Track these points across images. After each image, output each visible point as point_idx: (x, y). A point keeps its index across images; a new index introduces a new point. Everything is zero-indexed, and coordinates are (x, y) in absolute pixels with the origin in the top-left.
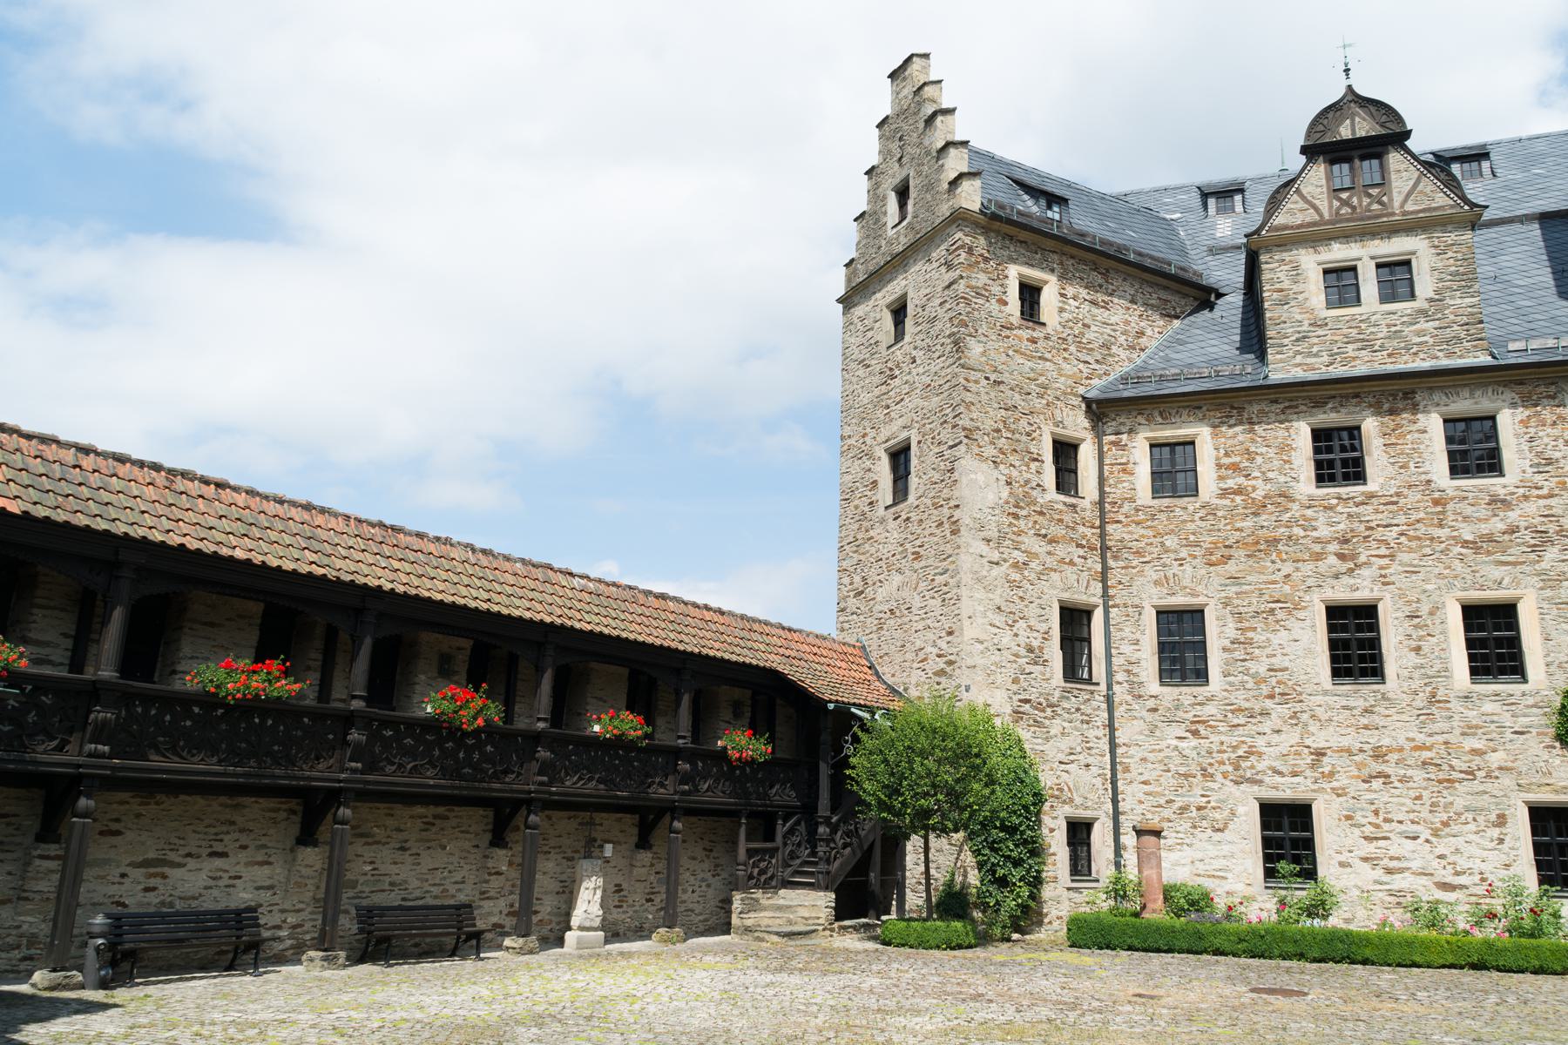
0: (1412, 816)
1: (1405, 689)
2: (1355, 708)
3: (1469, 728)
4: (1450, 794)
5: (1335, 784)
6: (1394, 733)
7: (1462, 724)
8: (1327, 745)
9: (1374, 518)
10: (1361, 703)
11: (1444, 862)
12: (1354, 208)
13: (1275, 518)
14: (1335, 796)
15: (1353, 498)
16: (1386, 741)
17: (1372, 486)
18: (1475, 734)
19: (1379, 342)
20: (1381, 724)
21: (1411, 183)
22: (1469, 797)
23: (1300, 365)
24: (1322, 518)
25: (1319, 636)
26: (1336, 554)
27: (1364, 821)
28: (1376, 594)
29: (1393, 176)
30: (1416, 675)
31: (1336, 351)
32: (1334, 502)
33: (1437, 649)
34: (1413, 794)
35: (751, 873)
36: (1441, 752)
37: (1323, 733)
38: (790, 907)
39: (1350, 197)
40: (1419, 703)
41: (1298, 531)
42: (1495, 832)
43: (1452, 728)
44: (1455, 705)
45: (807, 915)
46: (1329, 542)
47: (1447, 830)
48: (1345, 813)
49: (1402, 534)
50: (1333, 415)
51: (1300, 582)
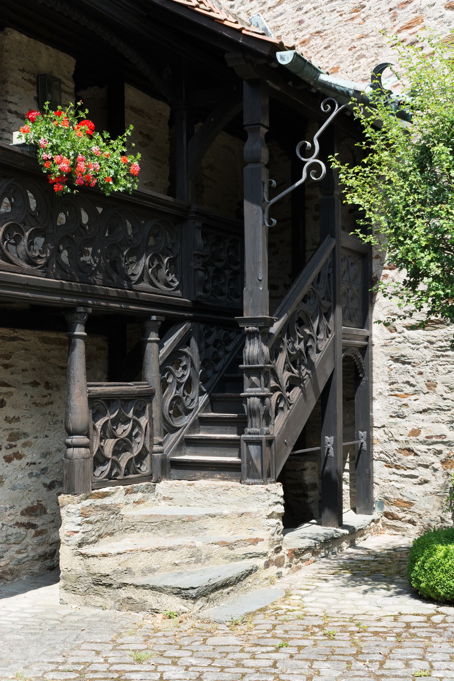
35: (101, 449)
38: (190, 520)
45: (230, 538)
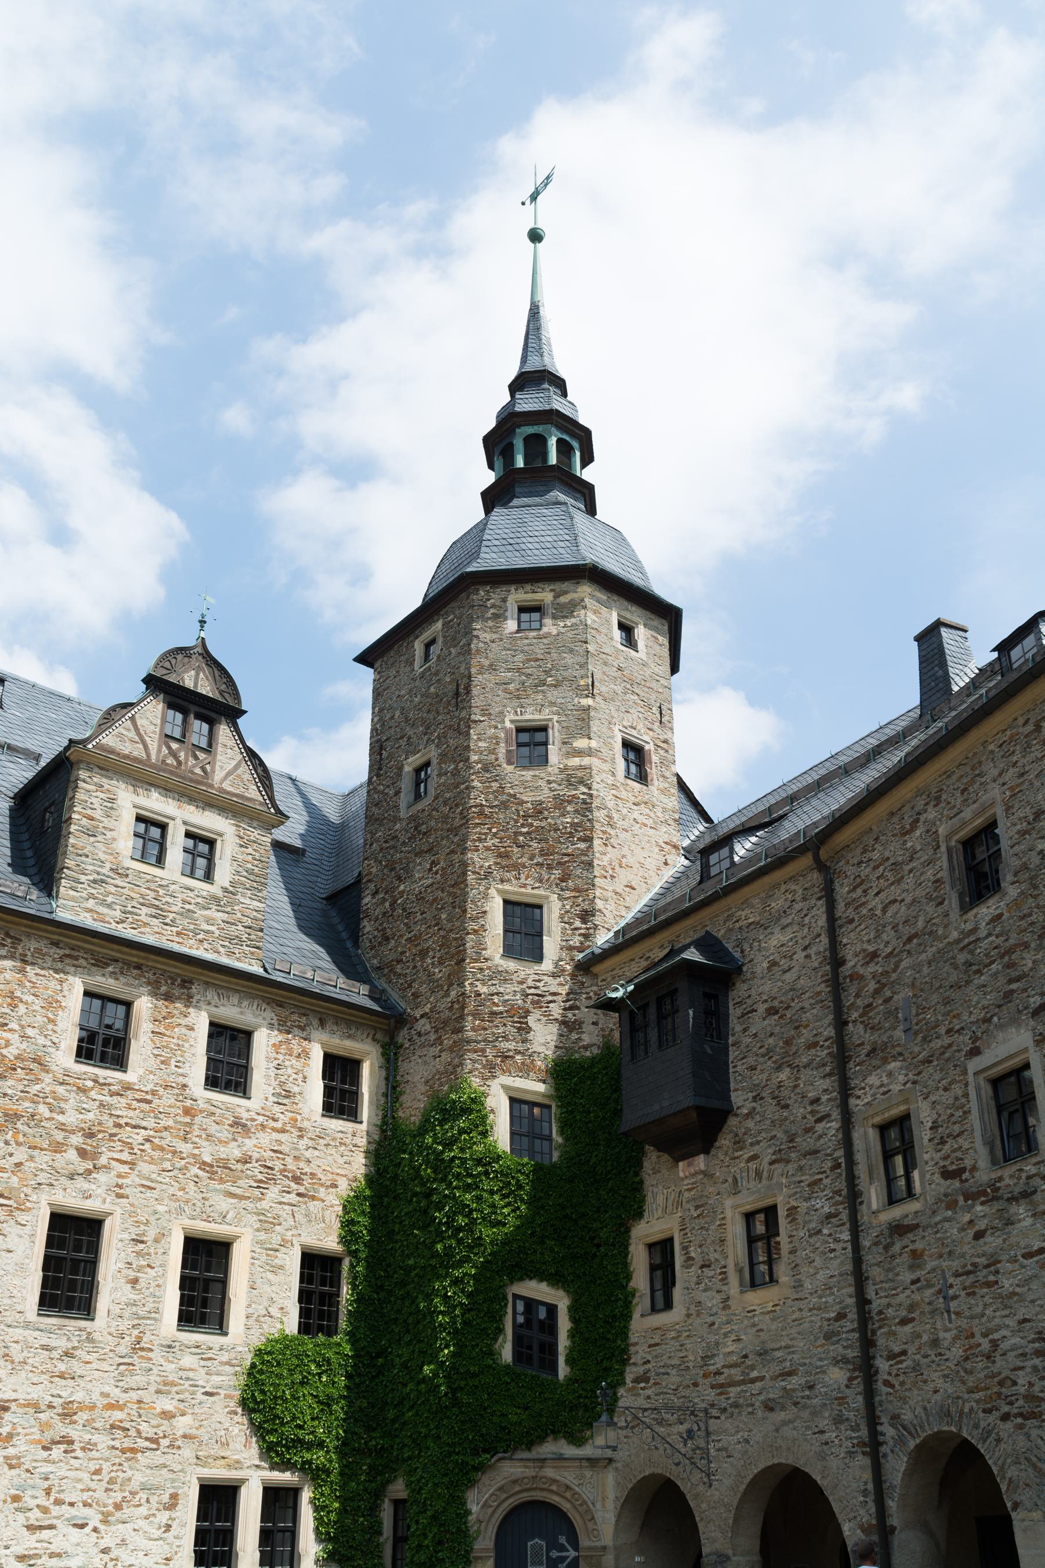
0: (85, 1496)
1: (113, 1330)
2: (54, 1348)
3: (165, 1384)
4: (130, 1468)
5: (11, 1451)
6: (89, 1386)
7: (158, 1379)
8: (14, 1396)
9: (124, 1114)
10: (62, 1344)
11: (106, 1558)
12: (179, 763)
13: (21, 1088)
14: (6, 1467)
15: (110, 1085)
16: (79, 1396)
17: (131, 1076)
18: (169, 1393)
19: (171, 916)
20: (79, 1372)
21: (234, 763)
22: (148, 1471)
23: (91, 911)
24: (73, 1099)
25: (36, 1250)
26: (77, 1149)
27: (32, 1503)
28: (107, 1207)
29: (220, 749)
30: (126, 1314)
31: (129, 909)
32: (90, 1084)
33: (153, 1284)
34: (93, 1466)
36: (134, 1412)
37: (13, 1379)
39: (179, 750)
40: (123, 1350)
41: (43, 1110)
42: (163, 1517)
43: (149, 1384)
44: (157, 1355)
46: (73, 1132)
47: (118, 1514)
48: (13, 1492)
49: (147, 1140)
50: (111, 981)
51: (31, 1176)
